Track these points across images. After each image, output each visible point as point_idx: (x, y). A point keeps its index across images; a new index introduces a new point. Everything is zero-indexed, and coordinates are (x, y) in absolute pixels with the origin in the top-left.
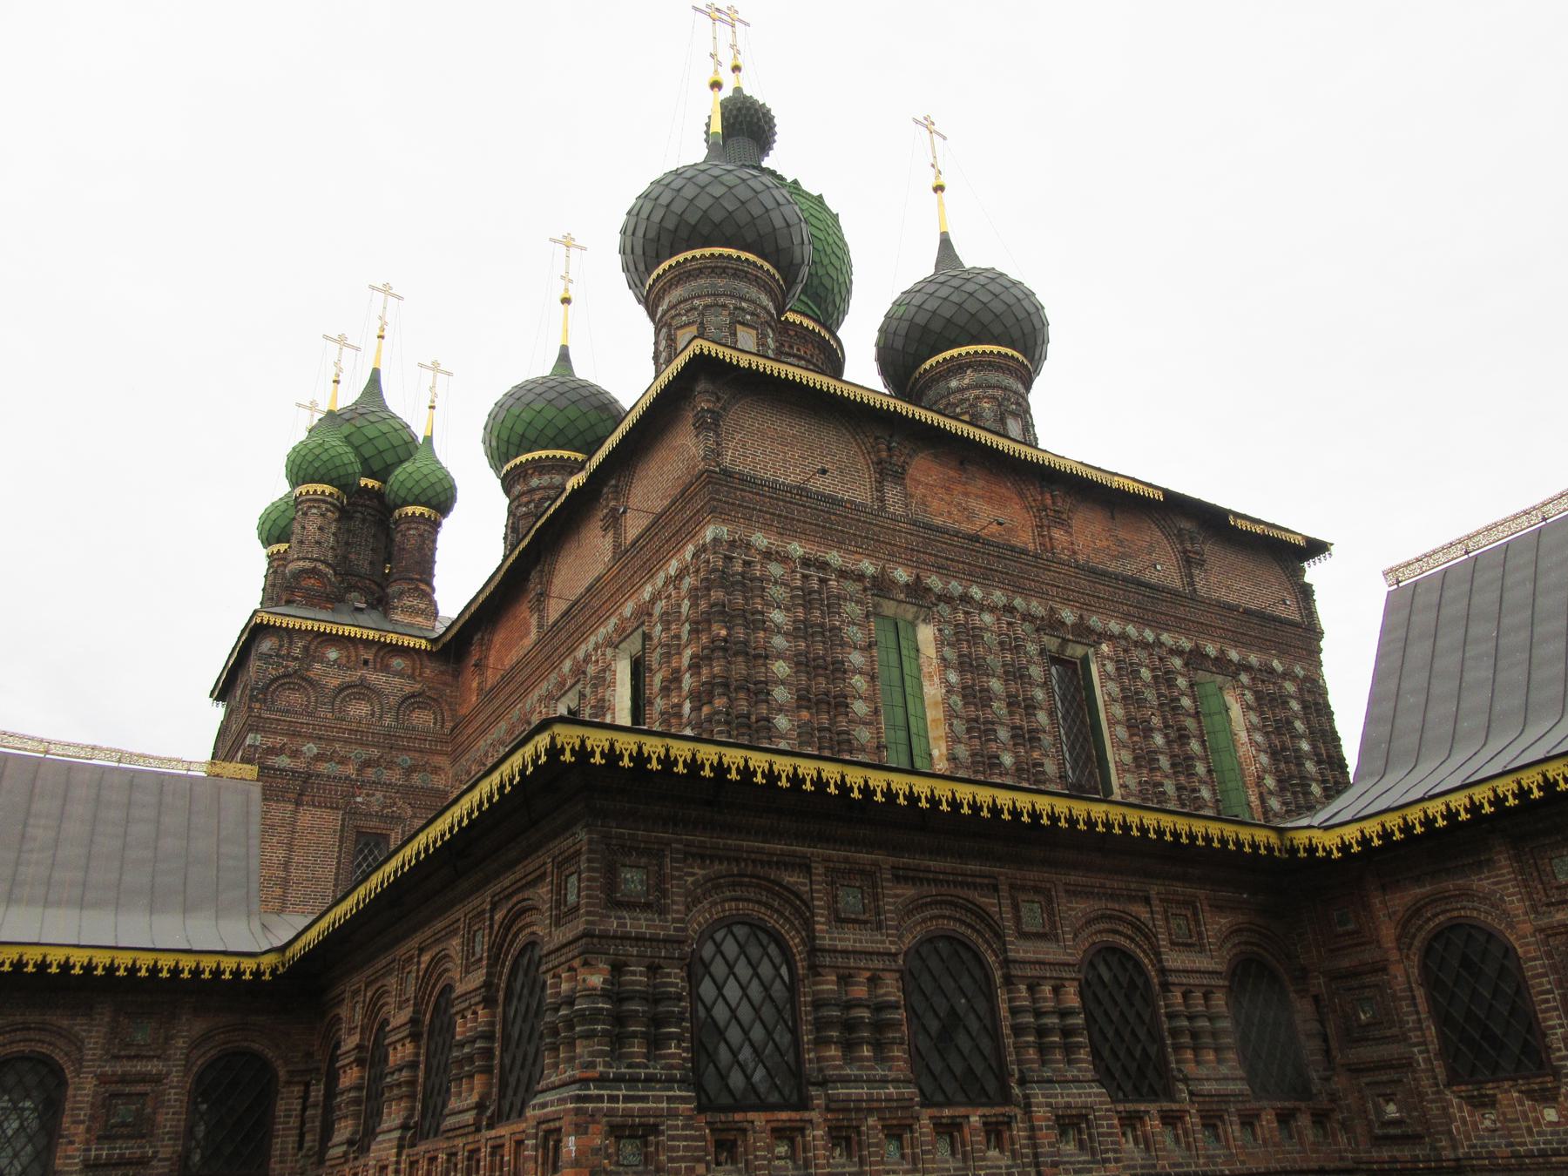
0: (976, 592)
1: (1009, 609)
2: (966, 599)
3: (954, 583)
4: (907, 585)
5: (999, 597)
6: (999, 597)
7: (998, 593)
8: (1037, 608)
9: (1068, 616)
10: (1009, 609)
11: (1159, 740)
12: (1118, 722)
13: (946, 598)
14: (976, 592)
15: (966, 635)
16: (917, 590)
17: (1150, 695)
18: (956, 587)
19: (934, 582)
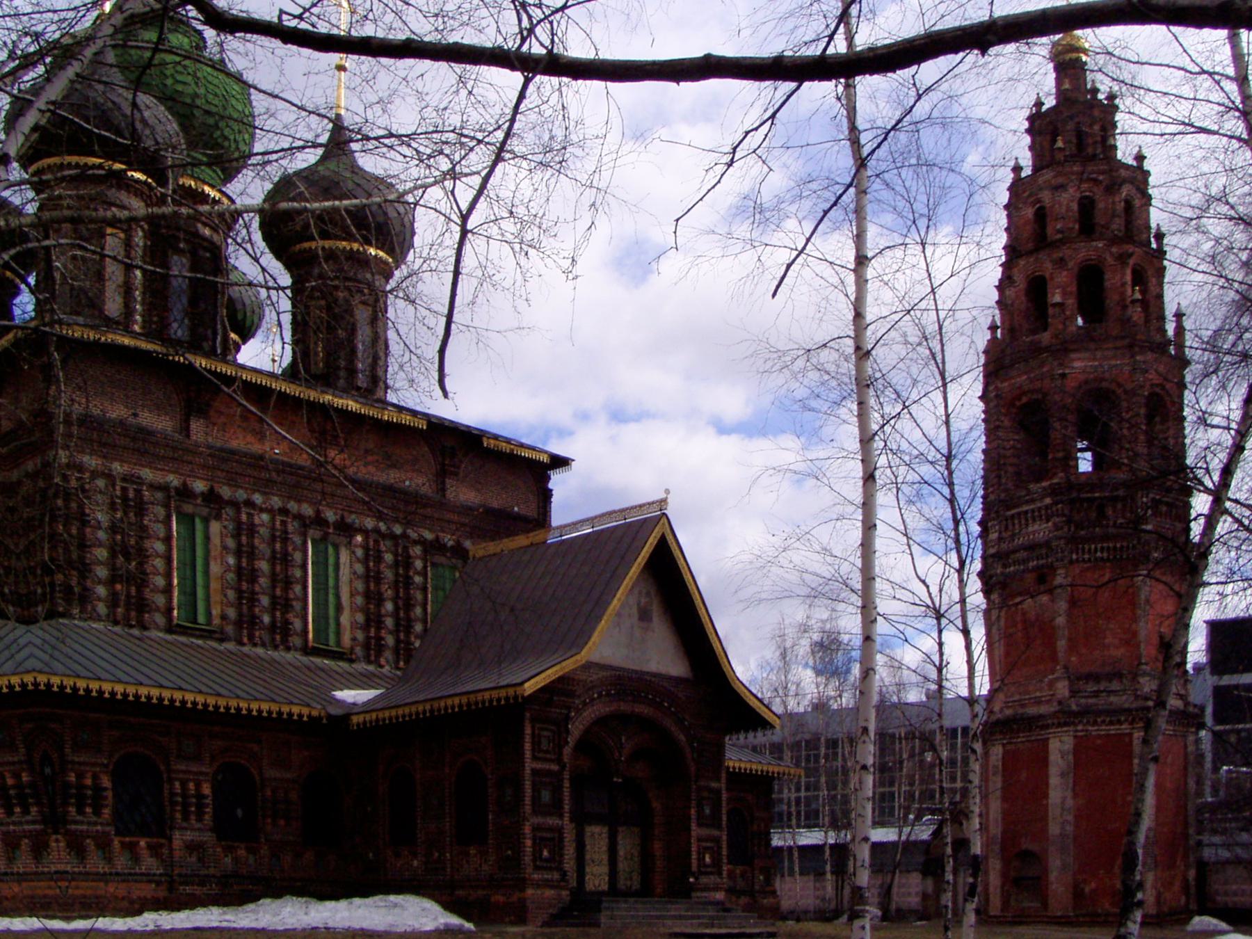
0: (258, 498)
1: (284, 511)
2: (249, 503)
3: (241, 491)
4: (203, 493)
5: (276, 502)
6: (276, 502)
7: (276, 499)
8: (308, 510)
9: (330, 516)
10: (284, 511)
11: (389, 606)
12: (358, 593)
13: (235, 504)
14: (258, 498)
15: (245, 530)
16: (211, 497)
17: (389, 574)
18: (241, 495)
19: (225, 492)
